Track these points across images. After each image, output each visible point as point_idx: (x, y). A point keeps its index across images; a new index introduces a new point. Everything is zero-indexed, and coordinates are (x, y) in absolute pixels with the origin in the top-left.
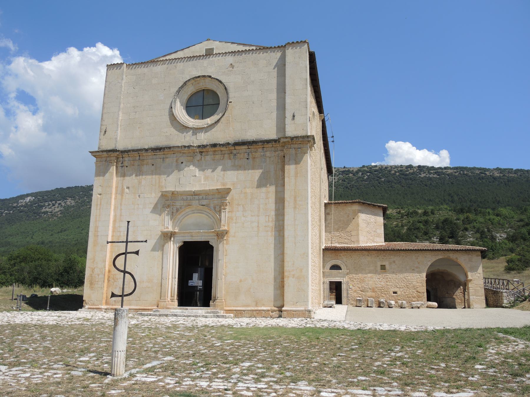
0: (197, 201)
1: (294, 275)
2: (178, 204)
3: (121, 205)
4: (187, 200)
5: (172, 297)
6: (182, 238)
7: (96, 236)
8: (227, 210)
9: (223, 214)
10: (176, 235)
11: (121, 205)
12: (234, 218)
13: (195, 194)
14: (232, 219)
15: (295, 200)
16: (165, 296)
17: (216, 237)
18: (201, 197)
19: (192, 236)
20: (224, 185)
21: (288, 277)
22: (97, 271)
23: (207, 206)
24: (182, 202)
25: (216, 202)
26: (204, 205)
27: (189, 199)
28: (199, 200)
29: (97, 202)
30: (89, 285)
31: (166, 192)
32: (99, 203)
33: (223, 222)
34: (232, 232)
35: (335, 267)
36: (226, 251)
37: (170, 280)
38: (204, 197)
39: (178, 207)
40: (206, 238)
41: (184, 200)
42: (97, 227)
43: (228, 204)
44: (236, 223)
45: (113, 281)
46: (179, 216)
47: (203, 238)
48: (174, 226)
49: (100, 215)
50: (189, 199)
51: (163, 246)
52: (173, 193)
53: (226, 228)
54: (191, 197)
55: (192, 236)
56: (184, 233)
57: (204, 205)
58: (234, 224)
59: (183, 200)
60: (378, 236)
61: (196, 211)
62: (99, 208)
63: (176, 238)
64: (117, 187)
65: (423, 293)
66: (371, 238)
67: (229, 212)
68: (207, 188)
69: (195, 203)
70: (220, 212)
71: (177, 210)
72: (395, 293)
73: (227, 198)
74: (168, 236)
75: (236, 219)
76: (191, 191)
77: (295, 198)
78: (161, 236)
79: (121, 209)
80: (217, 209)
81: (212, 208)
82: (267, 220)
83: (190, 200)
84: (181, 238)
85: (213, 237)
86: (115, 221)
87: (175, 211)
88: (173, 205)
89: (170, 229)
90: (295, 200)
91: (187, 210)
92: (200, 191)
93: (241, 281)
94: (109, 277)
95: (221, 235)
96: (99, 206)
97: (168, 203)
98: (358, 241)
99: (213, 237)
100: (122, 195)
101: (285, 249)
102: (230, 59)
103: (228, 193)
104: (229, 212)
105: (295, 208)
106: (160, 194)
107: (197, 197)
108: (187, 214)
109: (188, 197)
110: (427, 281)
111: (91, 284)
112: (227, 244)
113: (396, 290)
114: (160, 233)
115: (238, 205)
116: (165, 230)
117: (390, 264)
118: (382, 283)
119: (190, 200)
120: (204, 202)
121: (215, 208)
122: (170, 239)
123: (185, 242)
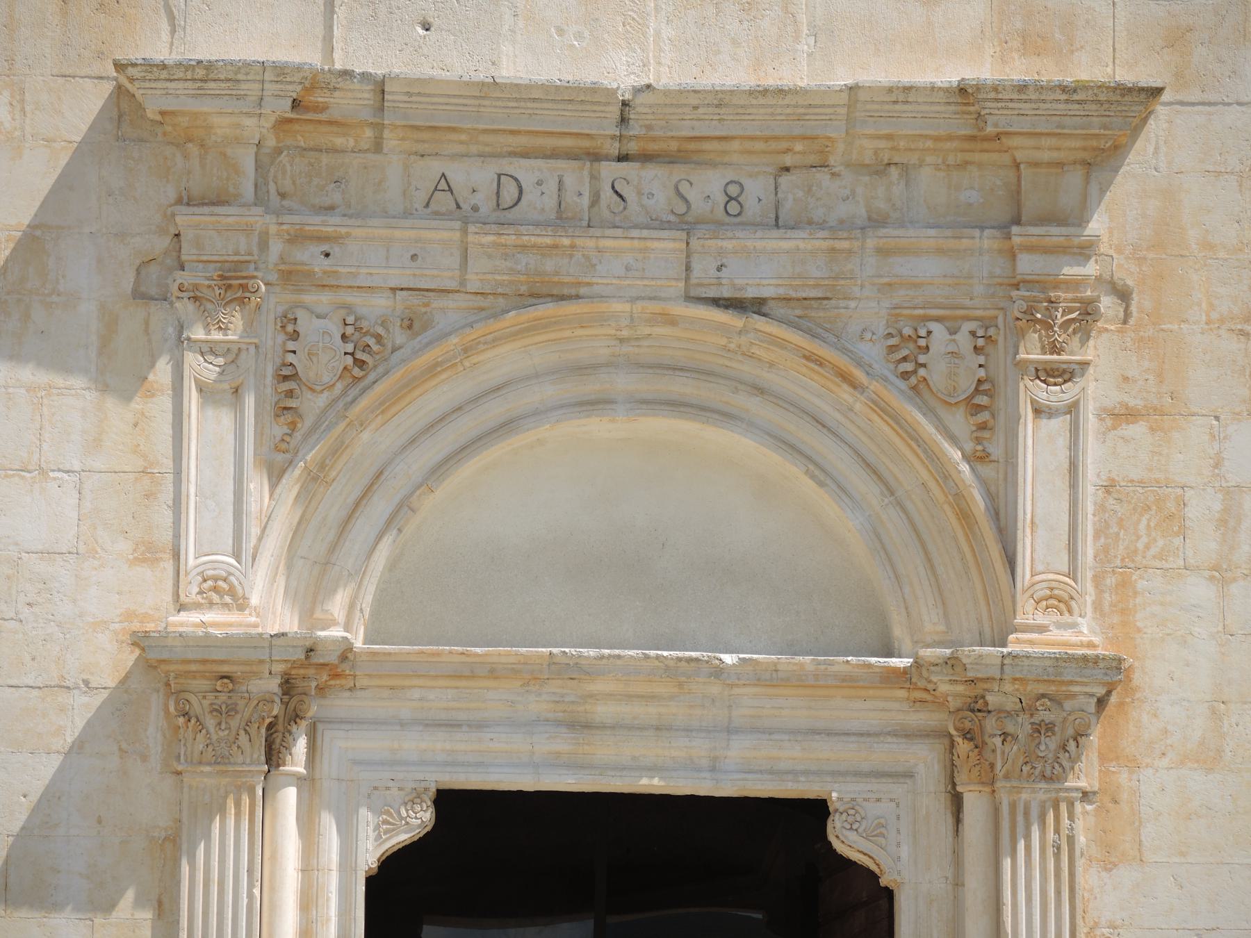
0: (668, 245)
2: (379, 262)
4: (506, 208)
6: (438, 744)
8: (1095, 391)
9: (1038, 448)
10: (340, 704)
12: (1202, 507)
13: (631, 139)
14: (1173, 521)
17: (925, 760)
18: (706, 187)
19: (581, 726)
20: (1032, 44)
23: (807, 311)
24: (448, 233)
25: (928, 268)
26: (756, 306)
27: (539, 201)
28: (685, 223)
31: (204, 74)
33: (1039, 553)
38: (756, 190)
39: (375, 306)
40: (791, 753)
41: (464, 215)
43: (1107, 304)
44: (1220, 574)
46: (374, 441)
47: (738, 750)
48: (314, 575)
50: (539, 201)
51: (171, 847)
52: (307, 102)
53: (1082, 633)
54: (575, 176)
55: (581, 726)
56: (468, 673)
57: (756, 306)
58: (1199, 590)
59: (444, 202)
61: (624, 383)
63: (337, 744)
67: (1122, 416)
68: (797, 72)
69: (632, 270)
70: (984, 407)
71: (363, 355)
73: (1097, 225)
74: (233, 712)
75: (1228, 521)
76: (591, 96)
78: (121, 708)
80: (937, 372)
81: (873, 351)
83: (562, 219)
84: (413, 744)
85: (887, 754)
87: (323, 358)
88: (291, 276)
89: (268, 609)
91: (504, 360)
92: (720, 100)
95: (1017, 733)
97: (214, 236)
99: (887, 754)
103: (1101, 160)
104: (1122, 416)
106: (84, 106)
107: (652, 185)
108: (495, 410)
109: (527, 171)
112: (1109, 861)
114: (108, 662)
116: (189, 621)
119: (562, 219)
120: (763, 263)
121: (908, 354)
122: (273, 756)
123: (447, 801)
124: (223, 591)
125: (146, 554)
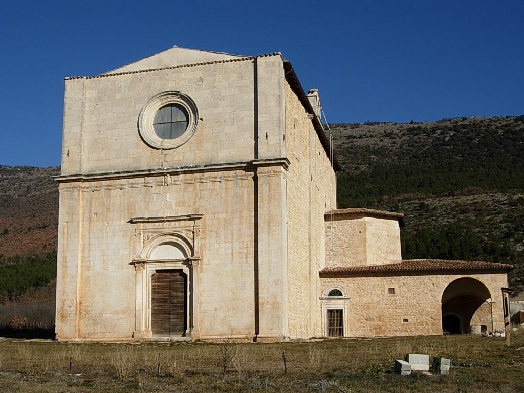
1: (268, 302)
3: (89, 233)
5: (146, 327)
7: (65, 267)
11: (89, 233)
12: (208, 245)
14: (206, 246)
15: (269, 226)
16: (139, 327)
21: (263, 304)
22: (67, 303)
29: (64, 231)
30: (60, 318)
32: (66, 232)
34: (205, 260)
35: (336, 293)
36: (201, 279)
37: (144, 311)
42: (65, 257)
44: (209, 250)
45: (85, 313)
49: (67, 245)
58: (208, 251)
60: (393, 252)
62: (66, 237)
64: (84, 214)
65: (438, 320)
66: (383, 255)
72: (406, 320)
75: (210, 246)
77: (269, 223)
79: (89, 238)
82: (241, 247)
86: (83, 250)
90: (269, 226)
93: (216, 309)
94: (80, 309)
96: (66, 235)
98: (365, 260)
100: (90, 223)
101: (259, 276)
102: (199, 72)
105: (269, 233)
110: (445, 306)
111: (63, 316)
113: (406, 317)
115: (211, 231)
117: (400, 287)
118: (391, 310)
124: (139, 256)
125: (134, 254)
